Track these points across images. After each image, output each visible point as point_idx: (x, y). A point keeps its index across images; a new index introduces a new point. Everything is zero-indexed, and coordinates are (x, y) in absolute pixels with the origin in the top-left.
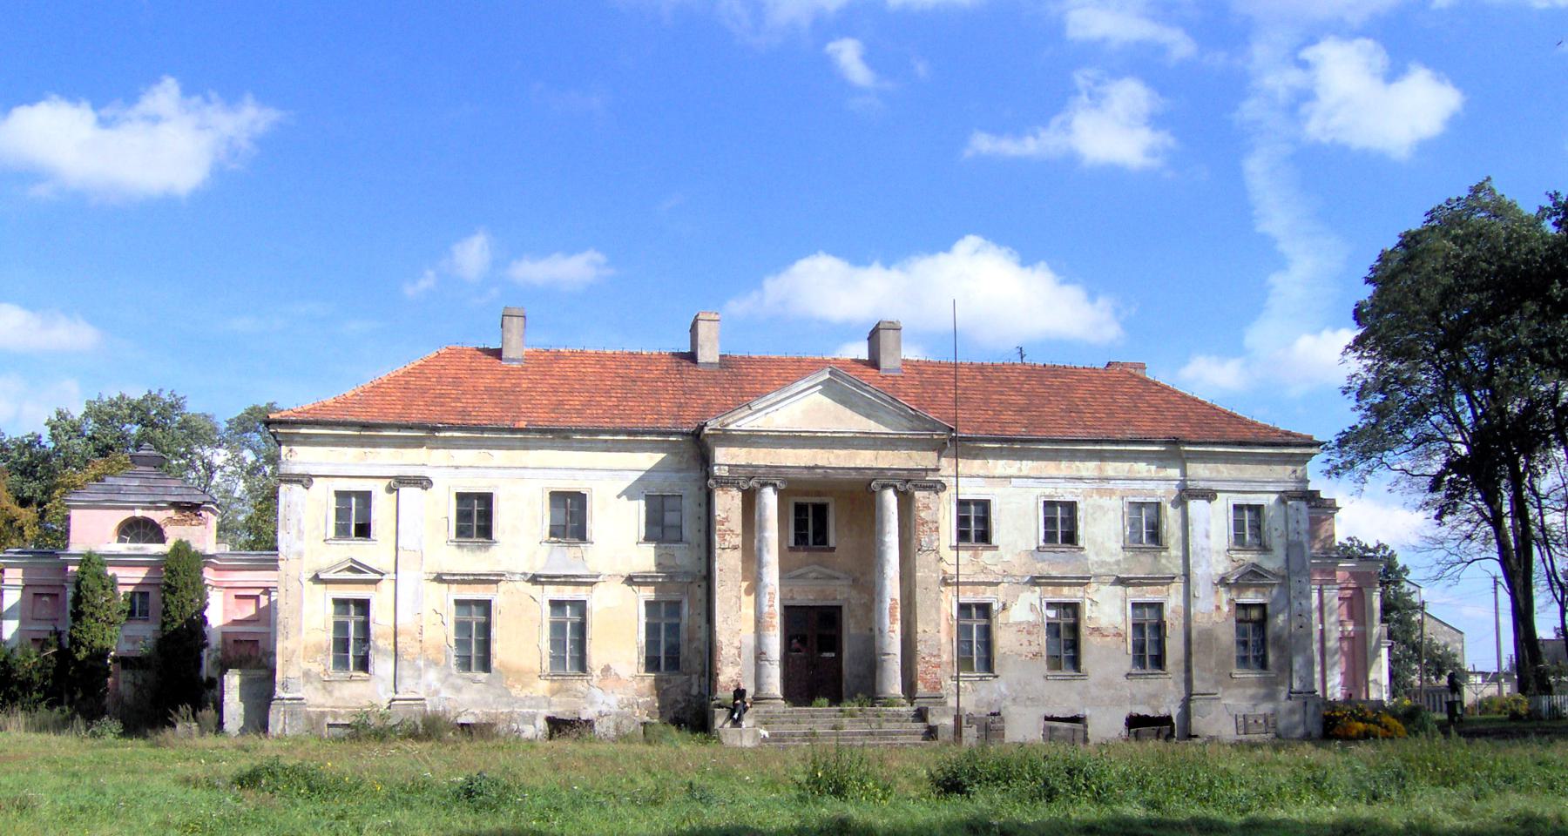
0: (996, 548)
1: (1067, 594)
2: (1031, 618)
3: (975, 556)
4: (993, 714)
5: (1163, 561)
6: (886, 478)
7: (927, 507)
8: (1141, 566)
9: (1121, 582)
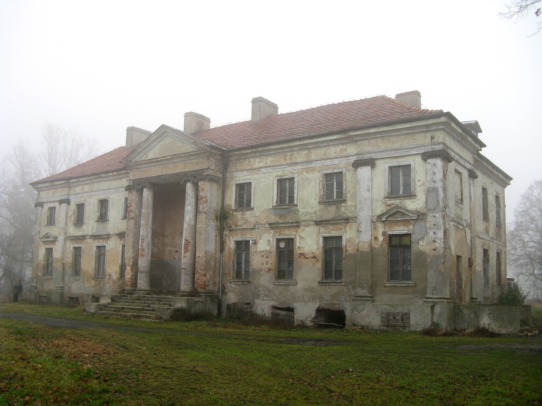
0: (253, 209)
1: (287, 234)
2: (268, 248)
3: (243, 215)
4: (247, 304)
5: (343, 209)
6: (186, 177)
7: (203, 190)
8: (331, 212)
9: (318, 223)
